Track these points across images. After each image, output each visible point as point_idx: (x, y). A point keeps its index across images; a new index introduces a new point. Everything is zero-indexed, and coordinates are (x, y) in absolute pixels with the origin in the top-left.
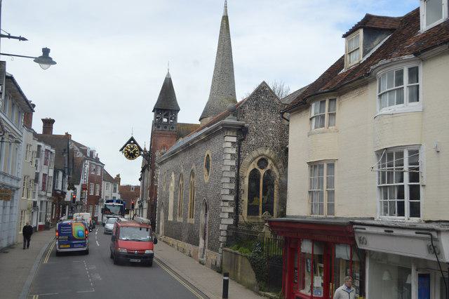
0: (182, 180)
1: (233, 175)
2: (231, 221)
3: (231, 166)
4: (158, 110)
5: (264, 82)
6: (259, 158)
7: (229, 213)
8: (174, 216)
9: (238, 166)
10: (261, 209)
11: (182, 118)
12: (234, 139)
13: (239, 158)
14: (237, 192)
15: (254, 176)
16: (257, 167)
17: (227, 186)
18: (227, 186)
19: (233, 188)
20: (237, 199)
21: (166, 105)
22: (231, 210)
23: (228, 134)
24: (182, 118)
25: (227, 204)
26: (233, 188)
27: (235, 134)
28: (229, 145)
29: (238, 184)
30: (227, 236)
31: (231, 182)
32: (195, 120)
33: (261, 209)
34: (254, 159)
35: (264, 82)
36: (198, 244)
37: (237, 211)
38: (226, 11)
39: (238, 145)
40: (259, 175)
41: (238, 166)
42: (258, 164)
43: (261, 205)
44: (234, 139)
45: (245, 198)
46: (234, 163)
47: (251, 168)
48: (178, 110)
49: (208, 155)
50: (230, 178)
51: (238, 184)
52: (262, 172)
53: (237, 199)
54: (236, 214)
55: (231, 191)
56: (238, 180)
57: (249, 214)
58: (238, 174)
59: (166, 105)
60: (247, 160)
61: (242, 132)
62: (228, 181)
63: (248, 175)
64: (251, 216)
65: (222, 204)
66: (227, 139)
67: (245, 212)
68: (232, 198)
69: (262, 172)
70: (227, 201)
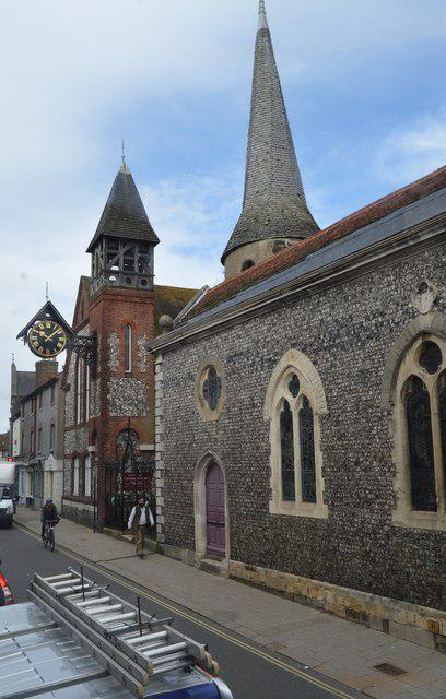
11: (169, 270)
21: (124, 237)
24: (169, 270)
32: (204, 274)
38: (262, 11)
48: (156, 242)
59: (124, 237)
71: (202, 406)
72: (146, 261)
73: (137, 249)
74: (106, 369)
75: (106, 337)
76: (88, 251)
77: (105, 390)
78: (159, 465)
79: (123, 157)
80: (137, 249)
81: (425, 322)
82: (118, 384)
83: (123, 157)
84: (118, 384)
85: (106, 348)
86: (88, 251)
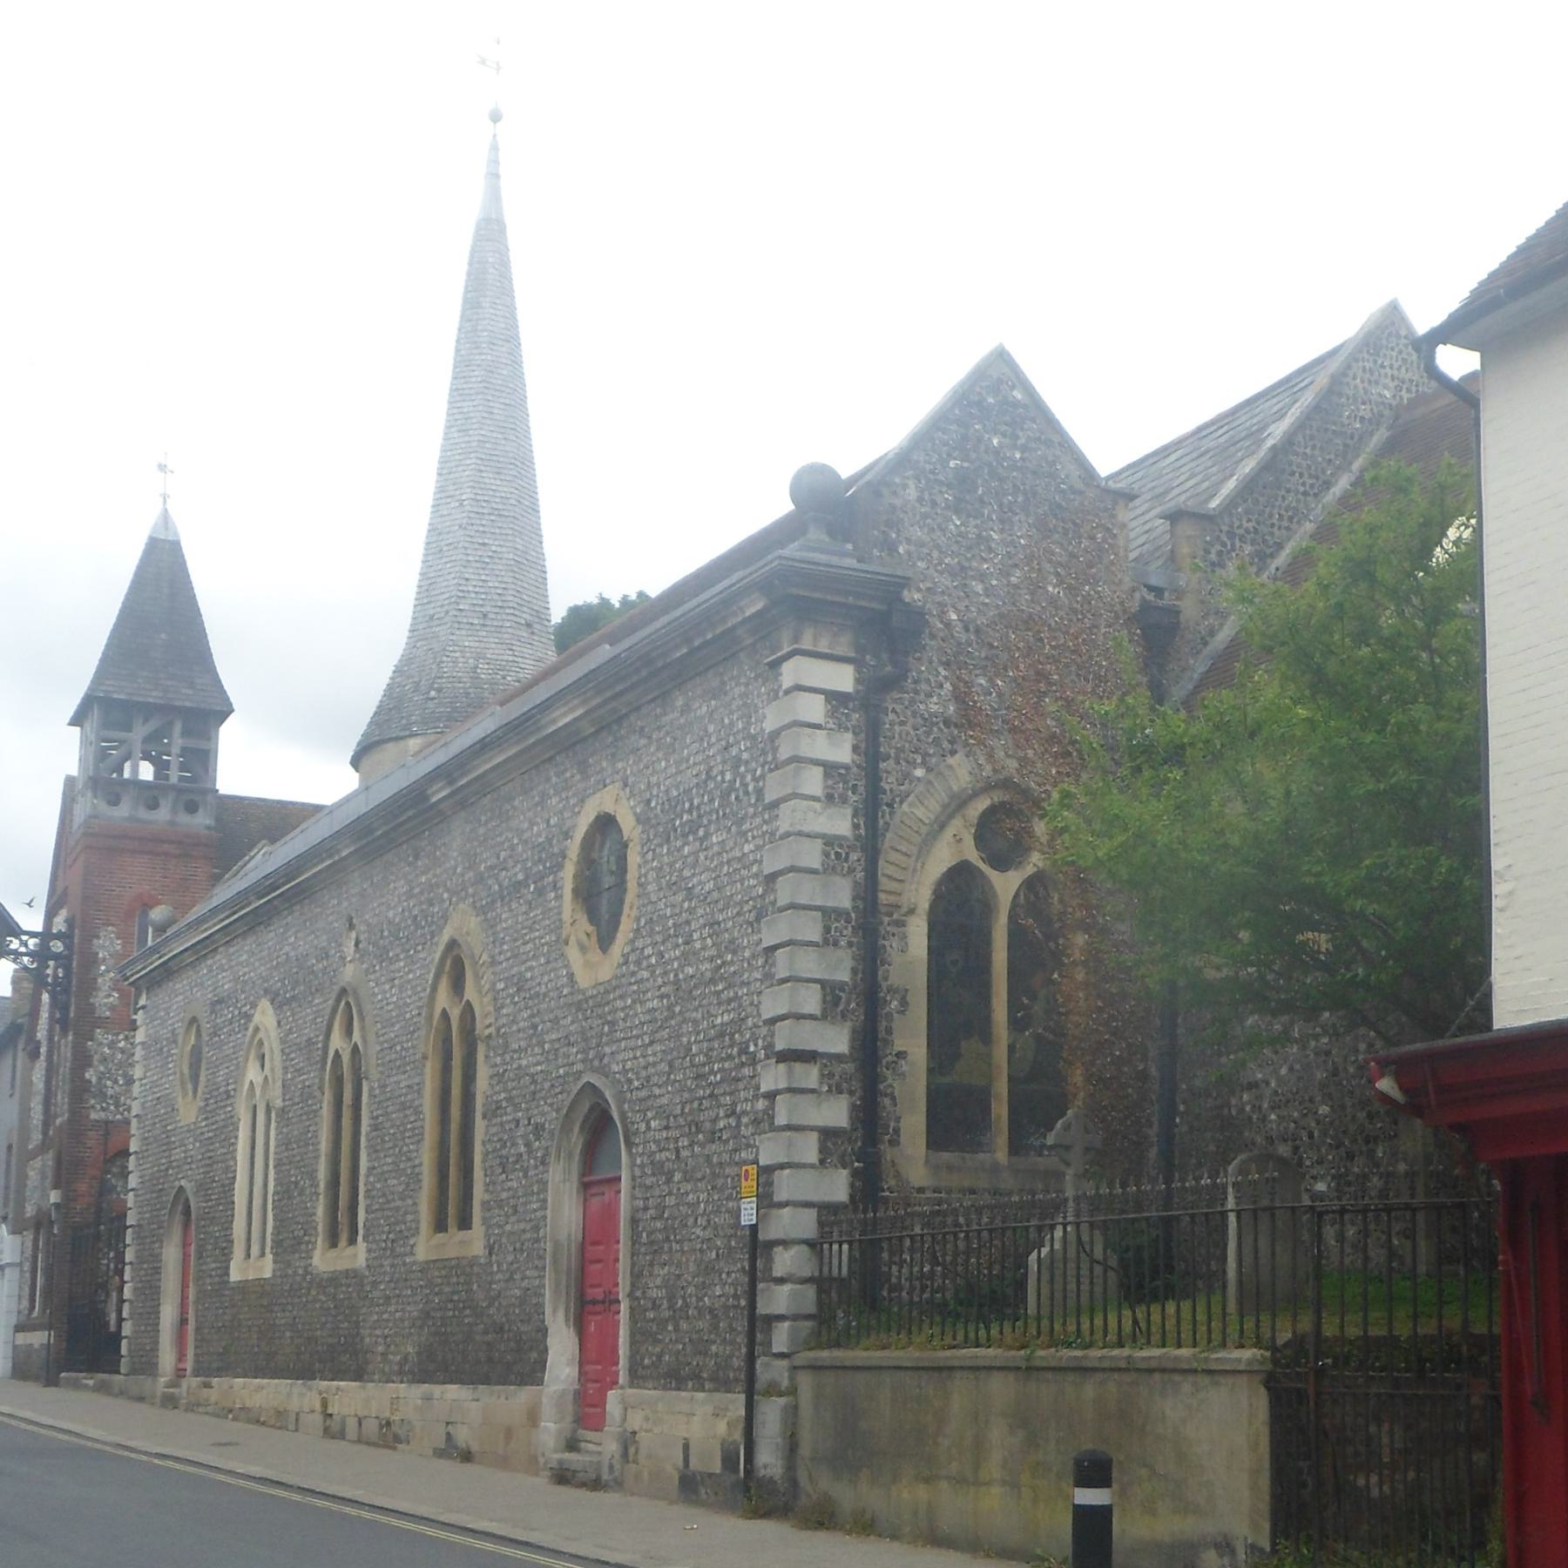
0: (349, 1032)
1: (842, 895)
2: (837, 1186)
3: (829, 841)
4: (107, 711)
5: (1001, 357)
6: (982, 804)
7: (827, 1134)
8: (289, 1244)
9: (870, 841)
10: (1000, 1110)
11: (248, 764)
12: (843, 679)
13: (869, 791)
14: (865, 1002)
15: (959, 901)
16: (973, 856)
17: (809, 964)
18: (809, 964)
19: (844, 976)
20: (870, 1049)
21: (156, 679)
22: (836, 1113)
23: (806, 644)
25: (810, 1076)
26: (844, 976)
27: (844, 647)
28: (813, 709)
29: (871, 958)
30: (821, 1283)
31: (828, 941)
32: (323, 779)
33: (1000, 1110)
34: (959, 803)
35: (1001, 357)
36: (532, 1373)
37: (871, 1120)
39: (864, 711)
40: (987, 907)
41: (870, 841)
42: (980, 840)
43: (1002, 1087)
44: (843, 679)
45: (911, 1040)
46: (840, 823)
47: (941, 860)
49: (605, 823)
50: (826, 912)
51: (871, 958)
52: (1006, 885)
53: (870, 1049)
54: (863, 1143)
55: (831, 992)
56: (868, 925)
57: (938, 1137)
58: (868, 893)
59: (156, 679)
60: (918, 810)
61: (883, 628)
62: (811, 930)
63: (921, 894)
64: (946, 1156)
65: (772, 1077)
66: (792, 671)
67: (913, 1123)
68: (836, 1040)
69: (1006, 885)
70: (808, 1057)
71: (185, 1095)
72: (201, 759)
73: (178, 728)
74: (88, 1010)
75: (90, 935)
76: (72, 723)
77: (82, 1060)
78: (131, 1220)
79: (165, 497)
80: (178, 728)
81: (349, 973)
82: (112, 1045)
83: (165, 497)
84: (112, 1045)
85: (90, 961)
86: (72, 723)
